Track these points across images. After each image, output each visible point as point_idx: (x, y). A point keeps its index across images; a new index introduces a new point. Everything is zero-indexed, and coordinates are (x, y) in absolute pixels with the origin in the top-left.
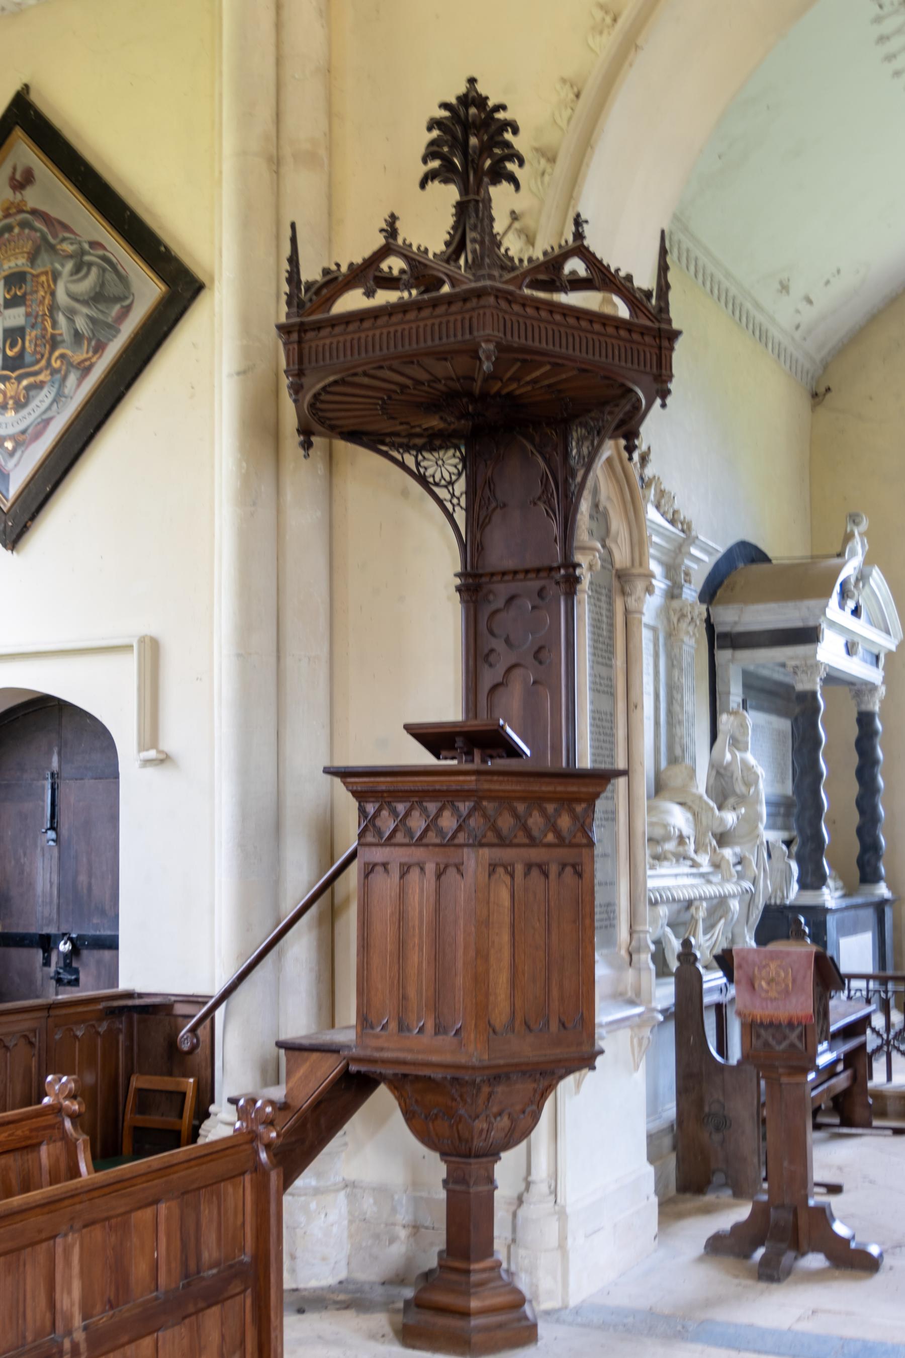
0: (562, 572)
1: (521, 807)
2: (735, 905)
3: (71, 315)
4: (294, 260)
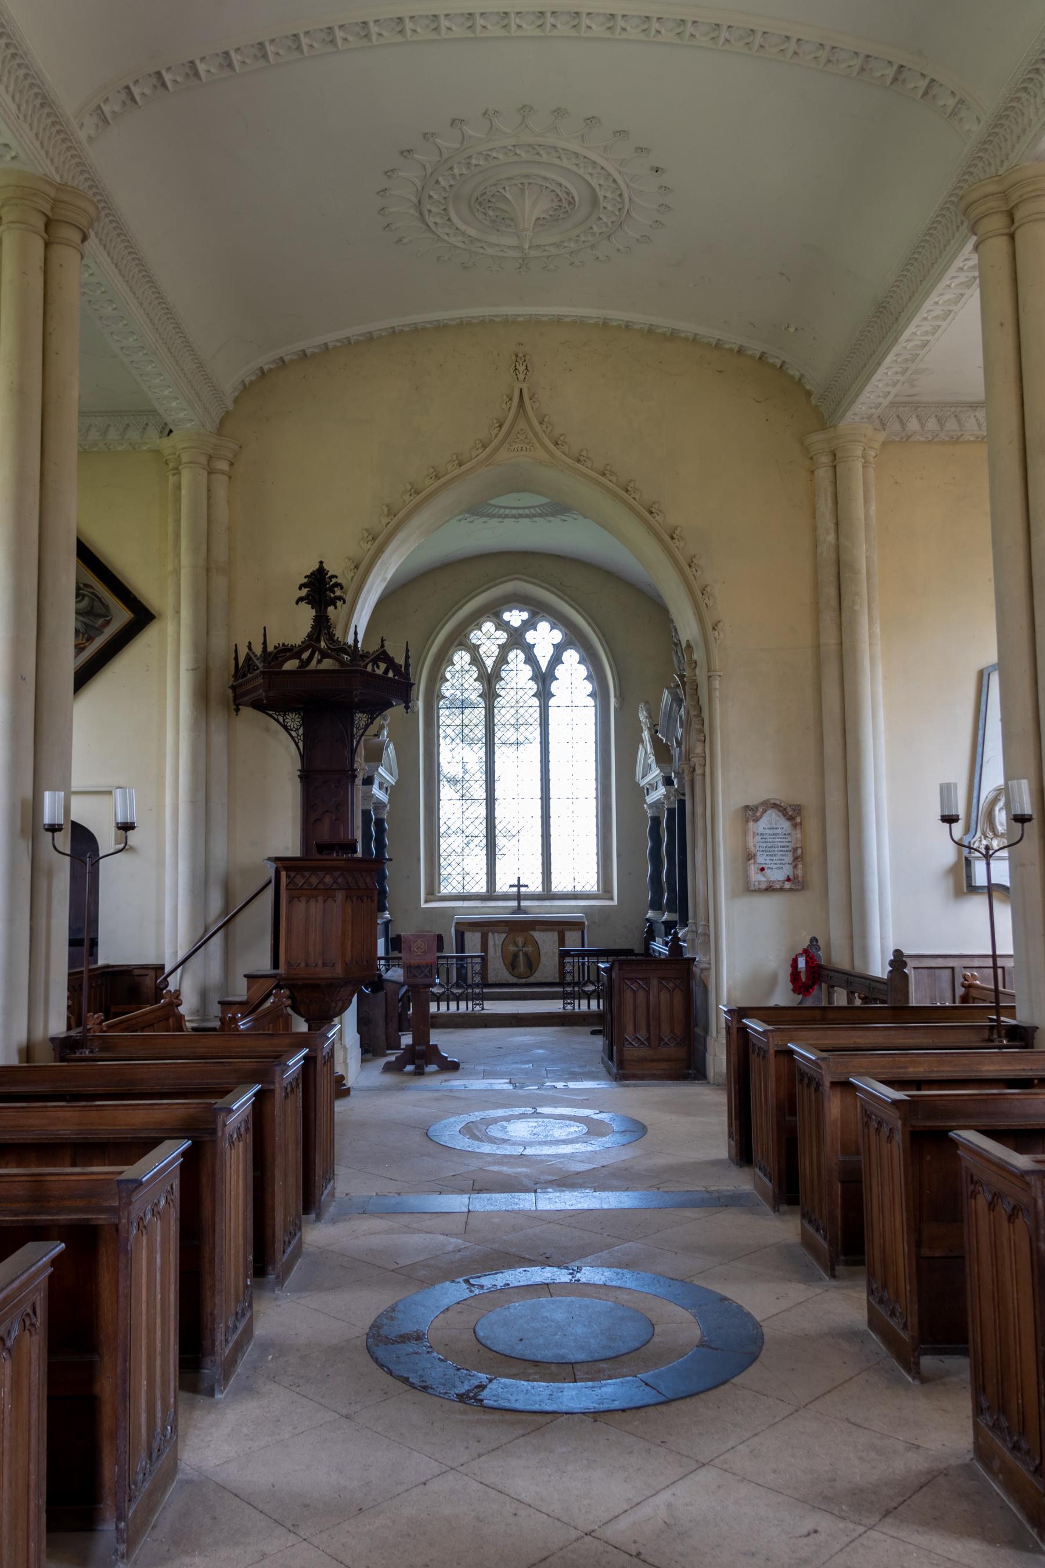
4: (265, 643)
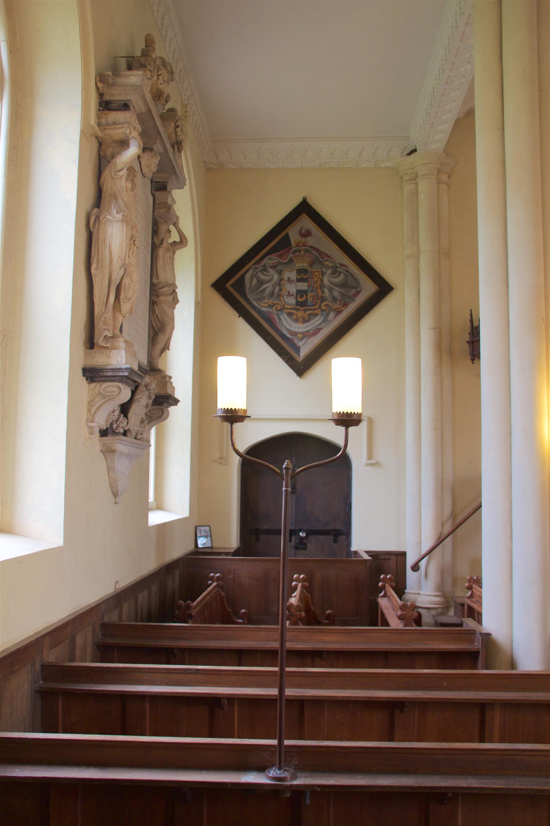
3: (331, 290)
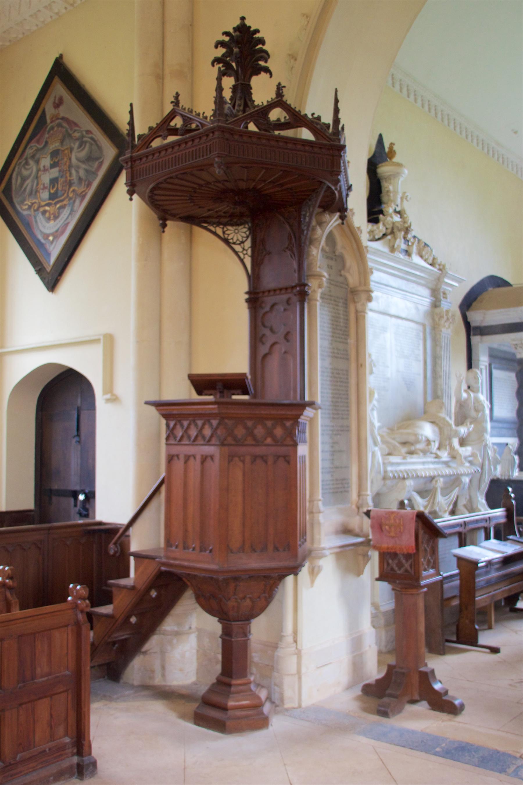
0: (298, 289)
1: (250, 423)
2: (466, 480)
